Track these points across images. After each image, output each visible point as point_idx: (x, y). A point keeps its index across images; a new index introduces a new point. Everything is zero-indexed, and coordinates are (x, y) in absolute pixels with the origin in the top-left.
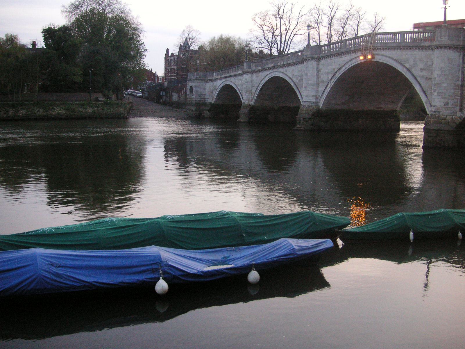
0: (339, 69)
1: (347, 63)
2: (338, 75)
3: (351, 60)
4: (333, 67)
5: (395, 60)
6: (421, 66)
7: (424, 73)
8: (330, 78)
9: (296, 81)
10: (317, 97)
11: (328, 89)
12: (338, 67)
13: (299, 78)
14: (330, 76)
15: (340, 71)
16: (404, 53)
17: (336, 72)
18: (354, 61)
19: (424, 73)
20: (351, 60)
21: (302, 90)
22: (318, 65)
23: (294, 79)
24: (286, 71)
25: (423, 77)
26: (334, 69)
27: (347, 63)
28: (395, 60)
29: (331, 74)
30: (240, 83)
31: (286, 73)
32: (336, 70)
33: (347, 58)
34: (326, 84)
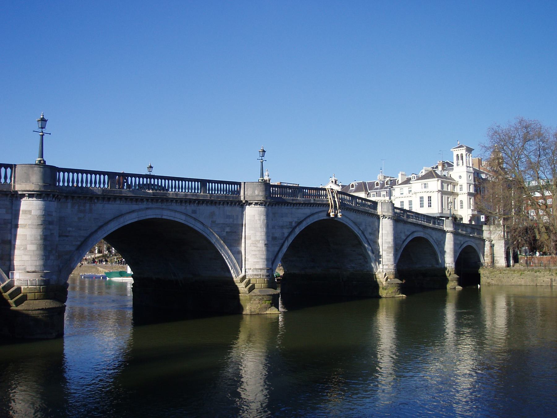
0: (299, 223)
1: (309, 216)
2: (297, 231)
3: (313, 214)
5: (355, 223)
8: (286, 235)
12: (296, 220)
13: (228, 229)
14: (286, 232)
16: (359, 217)
17: (295, 227)
18: (316, 216)
20: (313, 214)
24: (194, 212)
26: (291, 223)
28: (355, 223)
29: (288, 228)
31: (193, 215)
32: (294, 224)
34: (281, 241)
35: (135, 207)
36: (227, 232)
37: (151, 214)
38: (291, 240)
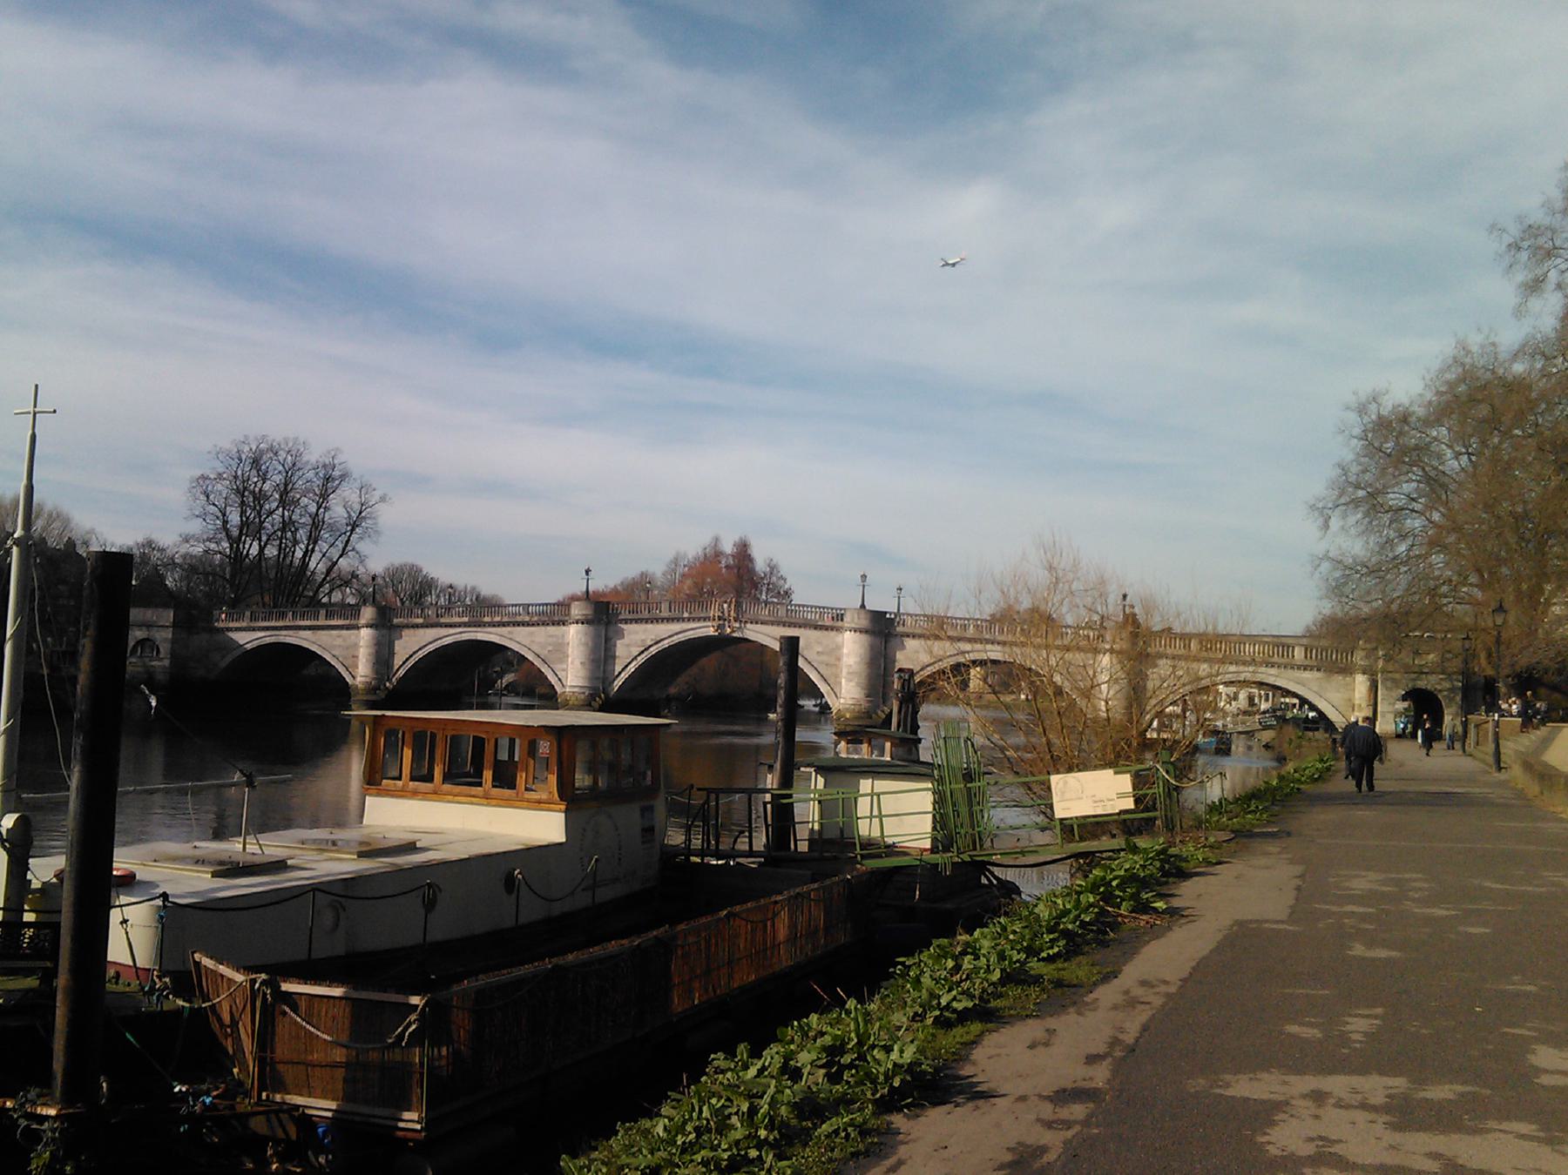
1: (677, 634)
2: (654, 650)
4: (643, 637)
6: (820, 649)
7: (824, 658)
9: (543, 653)
10: (603, 683)
11: (632, 668)
12: (653, 637)
13: (550, 648)
15: (660, 645)
19: (824, 658)
21: (557, 667)
22: (606, 631)
23: (534, 648)
25: (822, 663)
27: (677, 634)
30: (339, 642)
33: (676, 627)
35: (452, 631)
36: (549, 651)
37: (465, 637)
38: (641, 659)
